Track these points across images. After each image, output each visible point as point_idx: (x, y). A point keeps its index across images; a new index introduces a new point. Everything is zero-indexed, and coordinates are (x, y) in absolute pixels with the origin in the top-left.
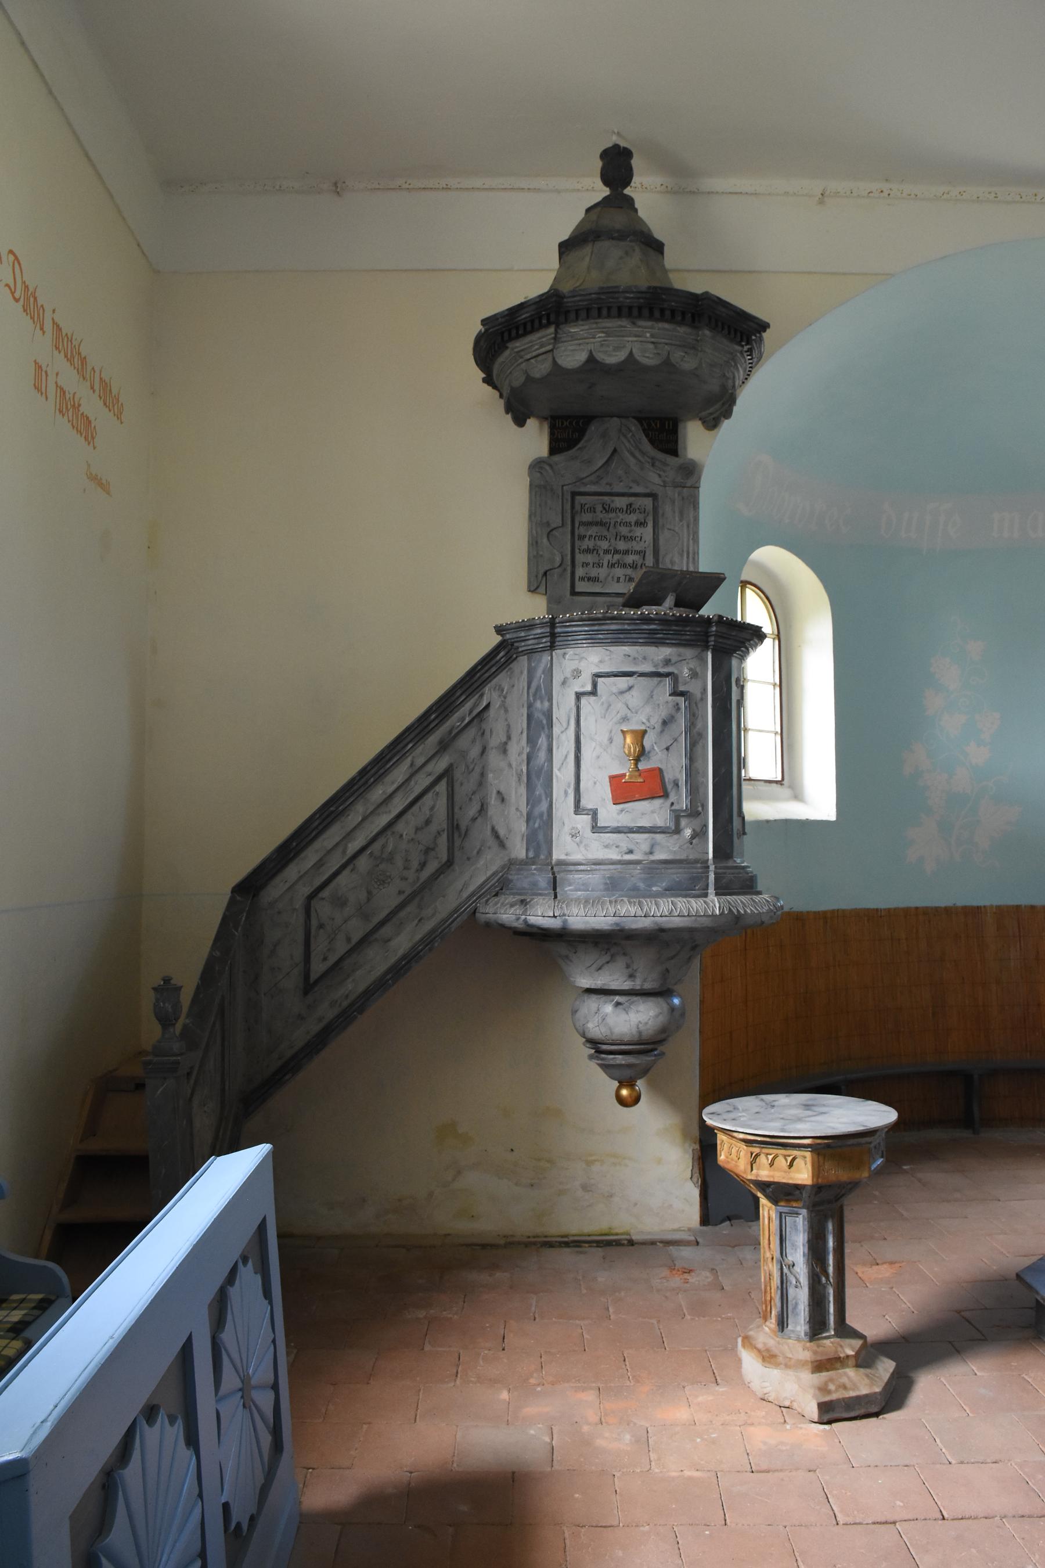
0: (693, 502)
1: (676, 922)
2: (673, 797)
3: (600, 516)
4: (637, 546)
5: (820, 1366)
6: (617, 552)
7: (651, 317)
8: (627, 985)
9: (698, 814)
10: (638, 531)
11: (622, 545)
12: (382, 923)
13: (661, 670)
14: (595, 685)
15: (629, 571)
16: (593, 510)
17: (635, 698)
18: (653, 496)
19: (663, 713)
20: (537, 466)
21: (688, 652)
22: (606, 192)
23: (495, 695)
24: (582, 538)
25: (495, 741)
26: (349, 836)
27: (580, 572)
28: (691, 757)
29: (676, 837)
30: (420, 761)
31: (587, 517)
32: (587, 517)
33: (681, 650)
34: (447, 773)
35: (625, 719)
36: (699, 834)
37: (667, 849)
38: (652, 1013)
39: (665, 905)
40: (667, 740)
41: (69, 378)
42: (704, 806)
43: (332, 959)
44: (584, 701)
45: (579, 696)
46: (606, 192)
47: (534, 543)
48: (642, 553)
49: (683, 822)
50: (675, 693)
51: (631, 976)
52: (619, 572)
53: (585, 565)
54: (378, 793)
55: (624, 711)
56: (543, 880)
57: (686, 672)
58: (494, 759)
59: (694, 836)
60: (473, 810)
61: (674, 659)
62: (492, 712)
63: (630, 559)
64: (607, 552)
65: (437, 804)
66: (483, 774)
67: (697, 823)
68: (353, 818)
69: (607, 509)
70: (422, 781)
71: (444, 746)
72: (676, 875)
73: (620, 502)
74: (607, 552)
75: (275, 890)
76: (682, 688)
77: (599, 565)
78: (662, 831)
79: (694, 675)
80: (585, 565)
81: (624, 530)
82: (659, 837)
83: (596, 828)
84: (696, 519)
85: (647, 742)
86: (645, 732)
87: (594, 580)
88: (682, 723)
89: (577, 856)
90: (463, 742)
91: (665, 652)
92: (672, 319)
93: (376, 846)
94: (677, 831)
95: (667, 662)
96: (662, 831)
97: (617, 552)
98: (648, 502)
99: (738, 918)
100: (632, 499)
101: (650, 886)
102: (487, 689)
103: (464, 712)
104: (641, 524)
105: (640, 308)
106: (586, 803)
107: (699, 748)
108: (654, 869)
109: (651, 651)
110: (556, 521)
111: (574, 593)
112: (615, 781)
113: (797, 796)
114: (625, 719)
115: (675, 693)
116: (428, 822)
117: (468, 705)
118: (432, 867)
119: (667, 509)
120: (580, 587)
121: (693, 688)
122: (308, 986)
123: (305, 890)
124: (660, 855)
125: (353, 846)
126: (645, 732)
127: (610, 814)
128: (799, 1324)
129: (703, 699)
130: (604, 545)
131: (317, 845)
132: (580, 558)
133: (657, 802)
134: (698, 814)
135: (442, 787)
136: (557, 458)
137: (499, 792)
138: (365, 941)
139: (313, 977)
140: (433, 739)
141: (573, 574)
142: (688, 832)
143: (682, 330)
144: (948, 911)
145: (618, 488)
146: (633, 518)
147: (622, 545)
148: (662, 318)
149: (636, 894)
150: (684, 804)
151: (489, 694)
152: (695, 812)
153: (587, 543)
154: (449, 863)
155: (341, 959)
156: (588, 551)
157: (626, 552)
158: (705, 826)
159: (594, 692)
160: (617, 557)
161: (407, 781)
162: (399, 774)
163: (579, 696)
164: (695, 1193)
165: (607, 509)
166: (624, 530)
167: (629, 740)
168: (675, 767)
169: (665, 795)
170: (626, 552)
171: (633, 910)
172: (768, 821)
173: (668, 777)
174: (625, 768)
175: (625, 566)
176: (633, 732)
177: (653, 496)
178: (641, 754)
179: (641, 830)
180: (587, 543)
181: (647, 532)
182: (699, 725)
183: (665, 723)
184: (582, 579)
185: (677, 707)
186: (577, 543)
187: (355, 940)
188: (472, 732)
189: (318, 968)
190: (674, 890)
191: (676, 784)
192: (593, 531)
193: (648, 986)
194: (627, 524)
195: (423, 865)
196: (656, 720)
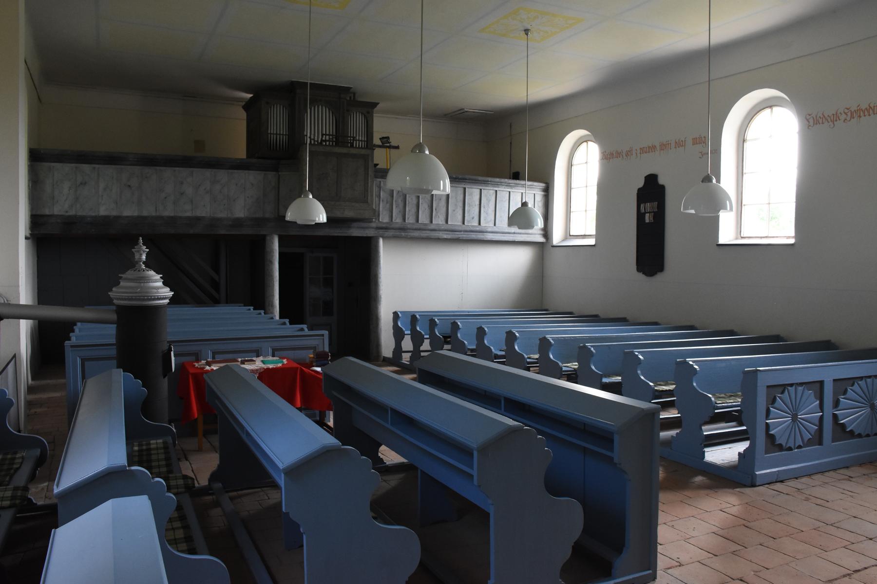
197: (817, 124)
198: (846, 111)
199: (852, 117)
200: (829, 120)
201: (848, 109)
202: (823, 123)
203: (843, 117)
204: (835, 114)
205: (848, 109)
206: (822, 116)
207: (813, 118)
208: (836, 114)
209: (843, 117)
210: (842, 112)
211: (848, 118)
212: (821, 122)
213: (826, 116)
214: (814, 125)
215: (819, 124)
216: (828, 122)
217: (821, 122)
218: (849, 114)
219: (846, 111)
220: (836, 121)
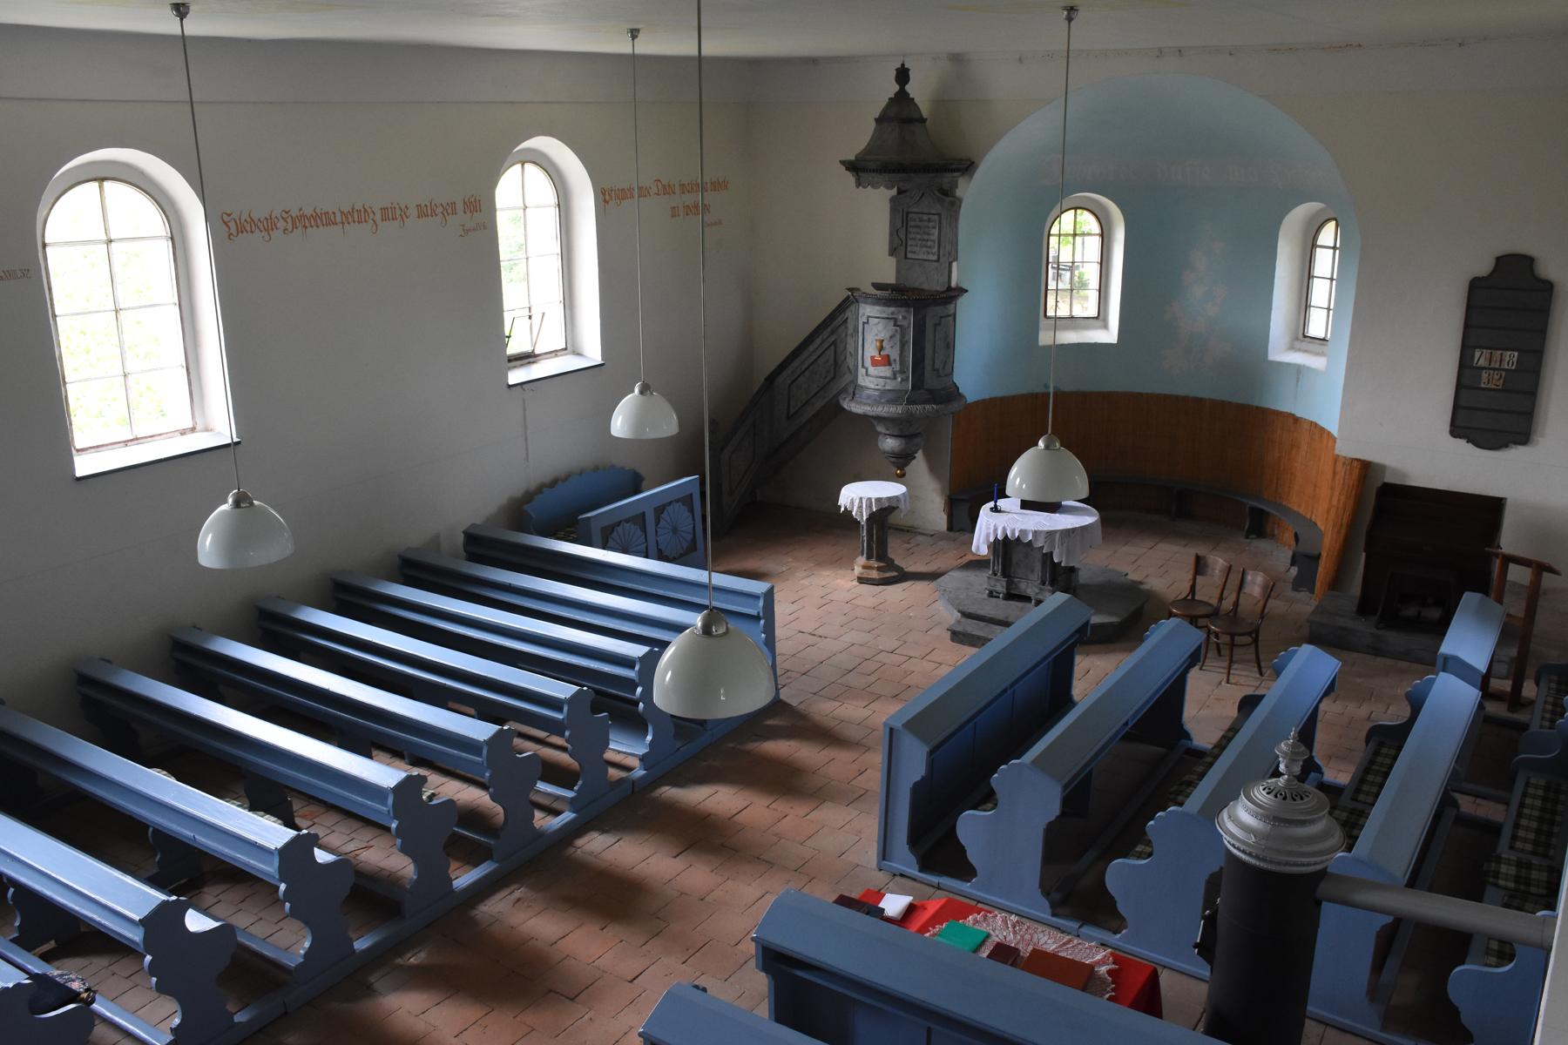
0: (956, 219)
1: (885, 415)
2: (893, 366)
3: (918, 223)
4: (932, 238)
5: (865, 567)
6: (924, 240)
7: (885, 172)
8: (887, 432)
9: (904, 372)
10: (933, 231)
11: (926, 237)
12: (812, 398)
13: (890, 316)
14: (868, 320)
15: (928, 249)
16: (915, 220)
17: (880, 327)
18: (939, 215)
19: (890, 333)
20: (892, 200)
21: (902, 309)
22: (897, 88)
23: (850, 314)
24: (910, 233)
25: (851, 331)
26: (803, 362)
27: (909, 249)
28: (902, 350)
29: (894, 381)
30: (825, 337)
31: (912, 223)
32: (912, 223)
33: (900, 309)
34: (834, 343)
35: (877, 335)
36: (905, 380)
37: (890, 385)
38: (897, 444)
39: (880, 409)
40: (892, 344)
41: (689, 199)
42: (908, 369)
43: (797, 408)
44: (866, 325)
45: (864, 323)
46: (897, 88)
47: (891, 235)
48: (934, 241)
49: (898, 375)
50: (895, 326)
51: (888, 429)
52: (924, 249)
53: (911, 245)
54: (811, 348)
55: (877, 332)
56: (851, 390)
57: (900, 317)
58: (849, 338)
59: (902, 380)
60: (843, 358)
61: (896, 312)
62: (849, 320)
63: (929, 243)
64: (920, 240)
65: (831, 352)
66: (846, 344)
67: (904, 376)
68: (803, 357)
69: (921, 220)
70: (826, 345)
71: (833, 332)
72: (891, 396)
73: (925, 217)
74: (920, 240)
75: (780, 380)
76: (899, 323)
77: (917, 246)
78: (889, 378)
79: (904, 318)
80: (911, 245)
81: (926, 230)
82: (888, 381)
83: (867, 374)
84: (956, 227)
85: (884, 344)
86: (883, 341)
87: (914, 252)
88: (898, 337)
89: (863, 384)
90: (840, 330)
91: (892, 309)
92: (894, 171)
93: (811, 368)
94: (895, 378)
95: (893, 313)
96: (889, 378)
97: (924, 240)
98: (936, 217)
99: (912, 415)
100: (931, 216)
101: (881, 399)
102: (847, 311)
103: (840, 320)
104: (934, 227)
105: (881, 170)
106: (866, 365)
107: (906, 347)
108: (884, 392)
109: (886, 308)
110: (899, 225)
111: (906, 257)
112: (872, 358)
113: (1105, 326)
114: (877, 335)
115: (895, 326)
116: (828, 361)
117: (841, 316)
118: (828, 379)
119: (944, 222)
120: (909, 255)
121: (905, 323)
122: (789, 418)
123: (789, 382)
124: (888, 388)
125: (804, 367)
126: (883, 341)
127: (872, 370)
128: (865, 555)
129: (909, 326)
130: (918, 236)
131: (792, 365)
132: (910, 242)
133: (888, 367)
134: (904, 372)
135: (832, 347)
136: (901, 196)
137: (850, 353)
138: (807, 402)
139: (791, 413)
140: (829, 329)
141: (906, 250)
142: (899, 379)
143: (900, 175)
144: (1185, 399)
145: (925, 211)
146: (931, 224)
147: (926, 237)
148: (889, 172)
149: (877, 402)
150: (897, 367)
151: (848, 314)
152: (902, 371)
153: (912, 236)
154: (834, 378)
155: (799, 409)
156: (912, 239)
157: (927, 240)
158: (909, 377)
159: (868, 323)
160: (924, 243)
161: (821, 344)
162: (818, 341)
163: (864, 323)
164: (945, 517)
165: (921, 220)
166: (926, 230)
167: (878, 344)
168: (894, 354)
169: (890, 364)
170: (927, 240)
171: (869, 409)
172: (1062, 345)
173: (892, 358)
174: (875, 353)
175: (927, 247)
176: (879, 340)
177: (939, 215)
178: (881, 349)
179: (881, 377)
180: (912, 236)
181: (936, 232)
182: (906, 338)
183: (891, 337)
184: (910, 252)
185: (896, 331)
186: (909, 235)
187: (804, 402)
188: (843, 327)
189: (792, 411)
190: (893, 402)
191: (895, 360)
192: (918, 230)
193: (895, 434)
194: (928, 227)
195: (826, 377)
196: (888, 336)
197: (242, 232)
198: (285, 215)
199: (295, 227)
200: (261, 227)
201: (287, 213)
202: (252, 232)
203: (281, 224)
204: (268, 217)
205: (287, 213)
206: (249, 220)
207: (236, 222)
208: (271, 219)
209: (281, 224)
210: (279, 216)
211: (290, 226)
212: (248, 229)
213: (256, 221)
214: (238, 234)
215: (247, 232)
216: (261, 231)
217: (248, 229)
218: (289, 220)
219: (285, 215)
220: (272, 229)
